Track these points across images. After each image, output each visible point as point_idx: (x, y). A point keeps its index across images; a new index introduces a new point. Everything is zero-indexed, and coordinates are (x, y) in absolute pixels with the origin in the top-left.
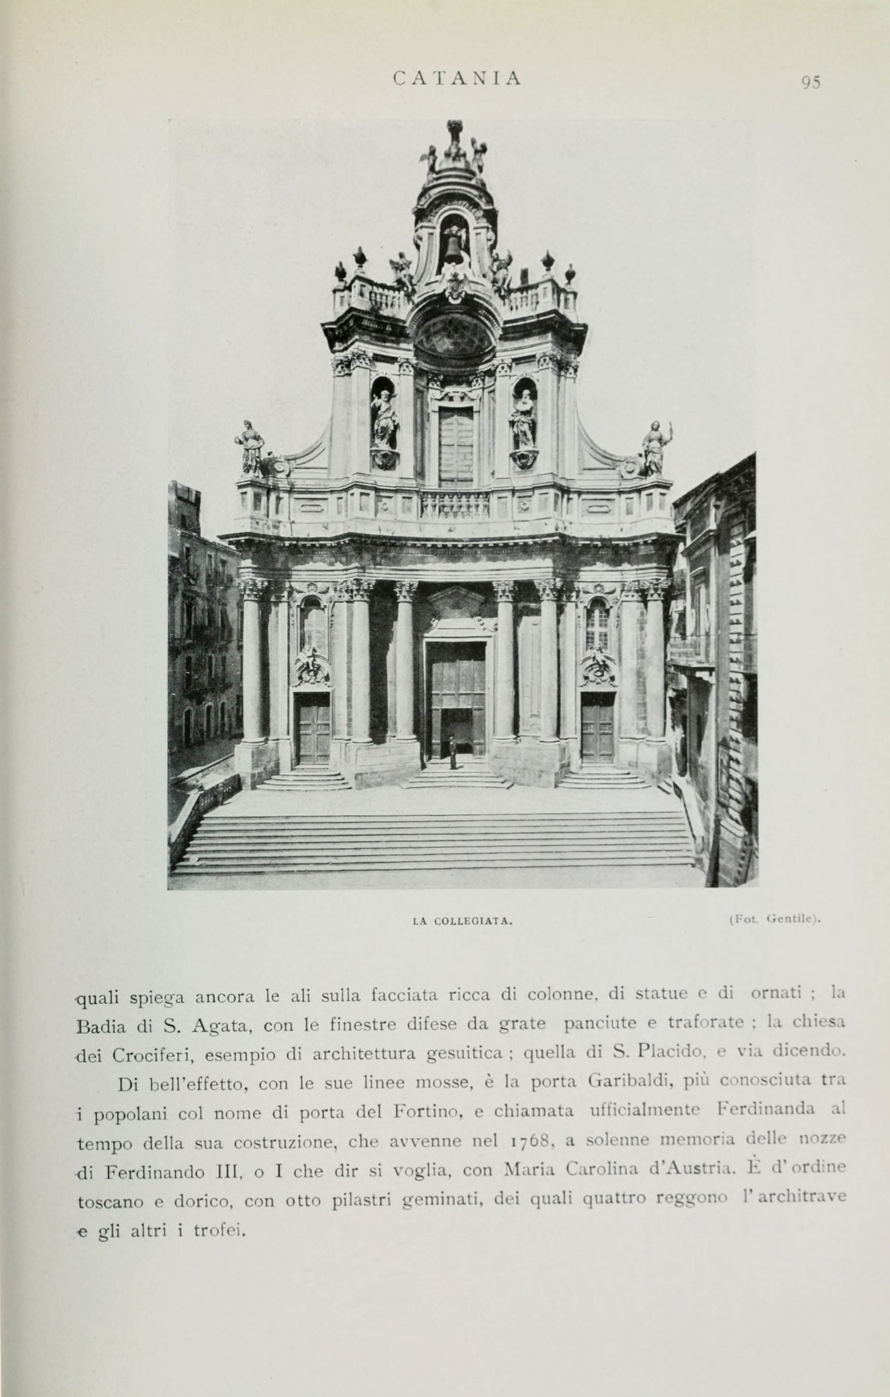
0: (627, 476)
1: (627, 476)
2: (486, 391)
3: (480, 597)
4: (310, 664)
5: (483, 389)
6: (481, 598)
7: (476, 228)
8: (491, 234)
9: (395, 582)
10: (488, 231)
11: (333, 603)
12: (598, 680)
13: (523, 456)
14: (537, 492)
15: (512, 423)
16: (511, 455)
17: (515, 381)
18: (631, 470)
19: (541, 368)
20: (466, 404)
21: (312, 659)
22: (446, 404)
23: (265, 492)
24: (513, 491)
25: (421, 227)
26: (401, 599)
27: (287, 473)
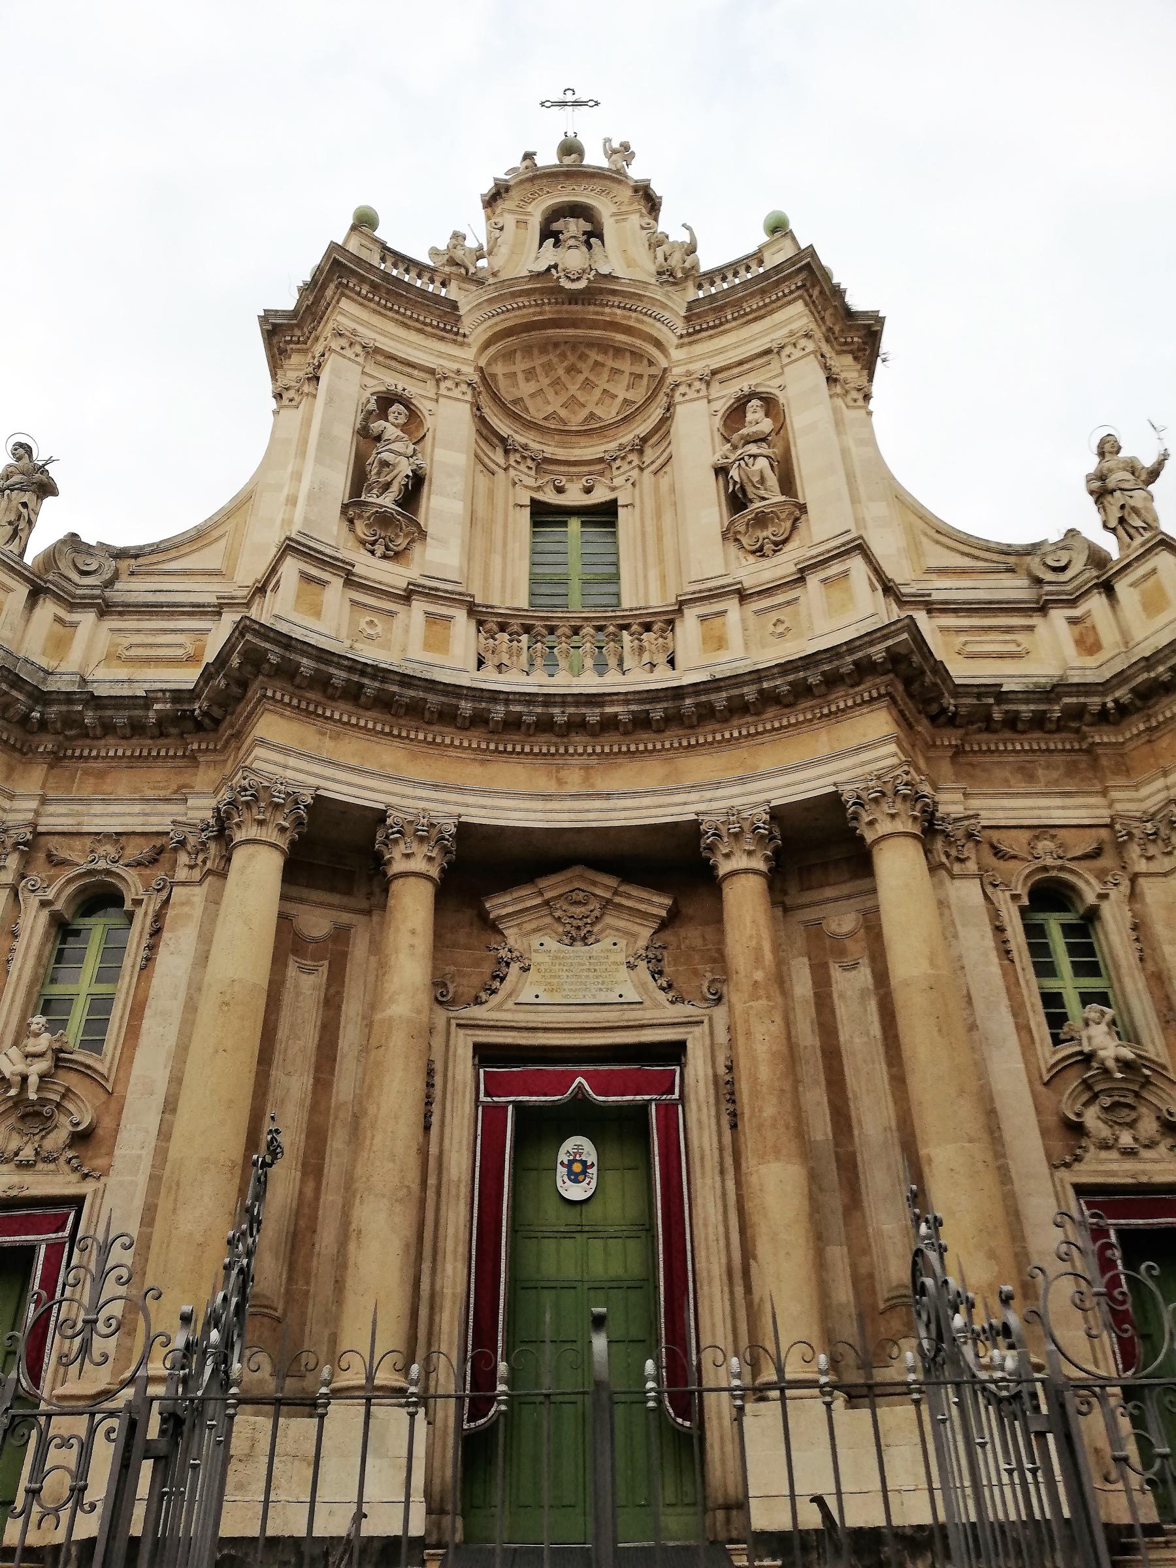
0: (1049, 576)
1: (1049, 576)
2: (647, 472)
3: (656, 899)
4: (33, 1080)
5: (642, 469)
6: (659, 904)
7: (614, 214)
8: (648, 219)
9: (380, 816)
10: (641, 216)
11: (164, 894)
12: (1126, 1139)
13: (761, 520)
14: (813, 580)
15: (721, 471)
16: (725, 536)
17: (722, 406)
18: (1062, 564)
19: (787, 360)
20: (600, 495)
21: (42, 1065)
22: (549, 497)
23: (23, 590)
24: (743, 596)
25: (504, 210)
26: (398, 866)
27: (107, 576)
